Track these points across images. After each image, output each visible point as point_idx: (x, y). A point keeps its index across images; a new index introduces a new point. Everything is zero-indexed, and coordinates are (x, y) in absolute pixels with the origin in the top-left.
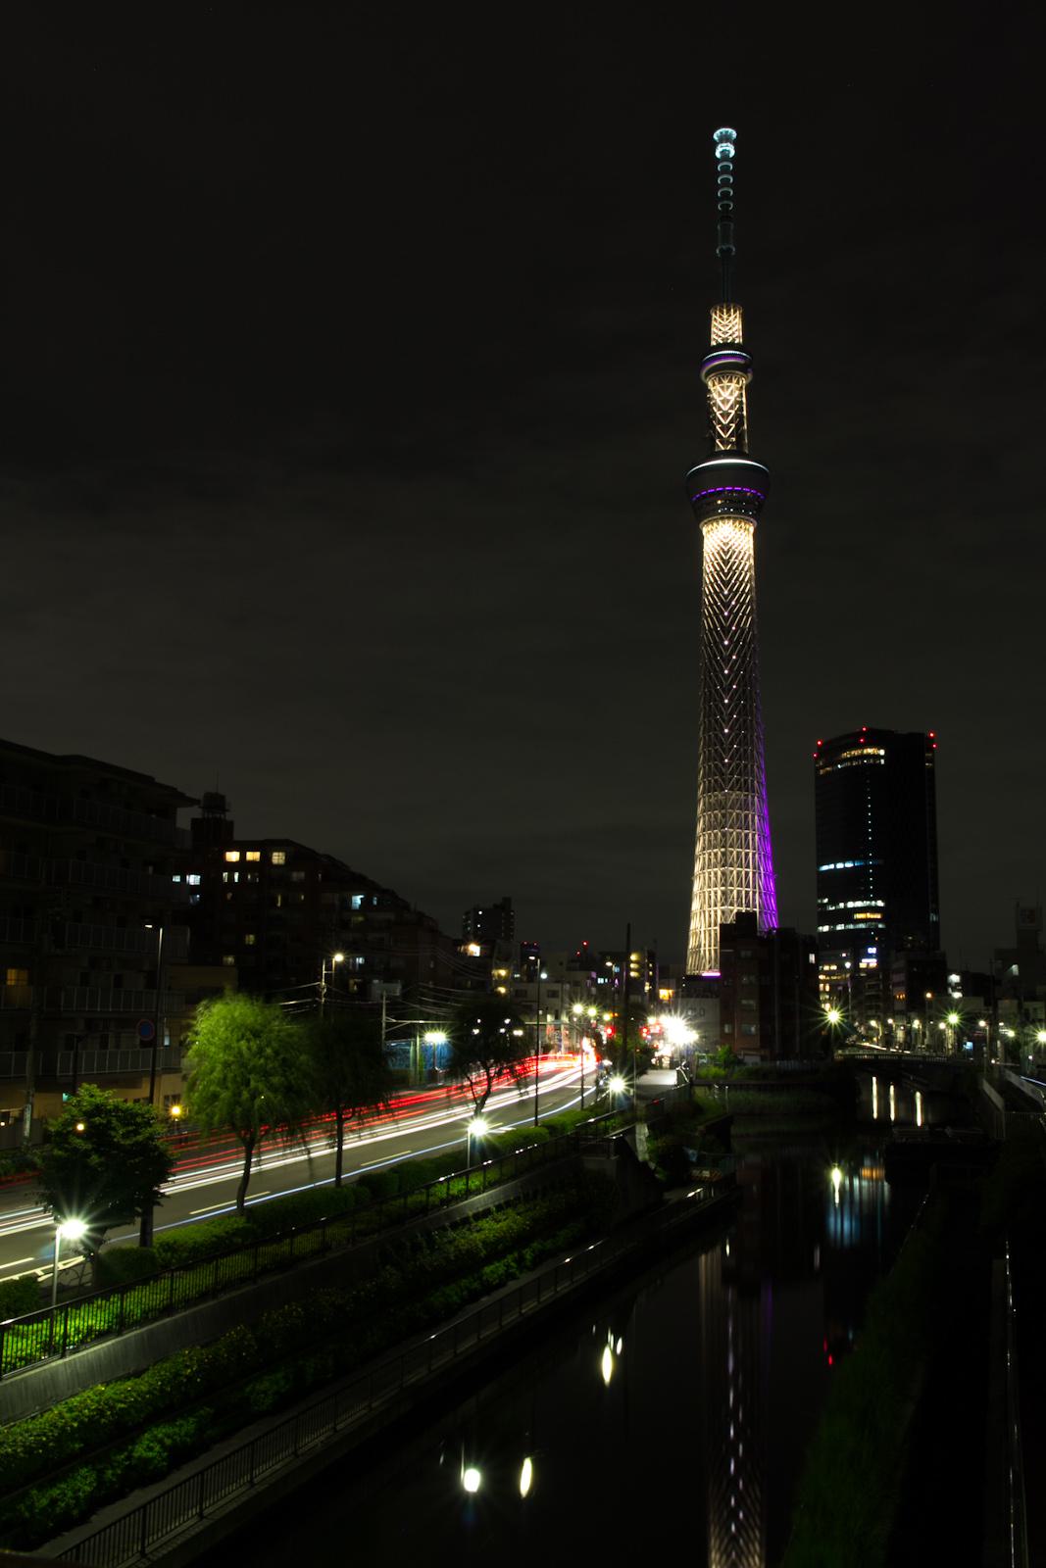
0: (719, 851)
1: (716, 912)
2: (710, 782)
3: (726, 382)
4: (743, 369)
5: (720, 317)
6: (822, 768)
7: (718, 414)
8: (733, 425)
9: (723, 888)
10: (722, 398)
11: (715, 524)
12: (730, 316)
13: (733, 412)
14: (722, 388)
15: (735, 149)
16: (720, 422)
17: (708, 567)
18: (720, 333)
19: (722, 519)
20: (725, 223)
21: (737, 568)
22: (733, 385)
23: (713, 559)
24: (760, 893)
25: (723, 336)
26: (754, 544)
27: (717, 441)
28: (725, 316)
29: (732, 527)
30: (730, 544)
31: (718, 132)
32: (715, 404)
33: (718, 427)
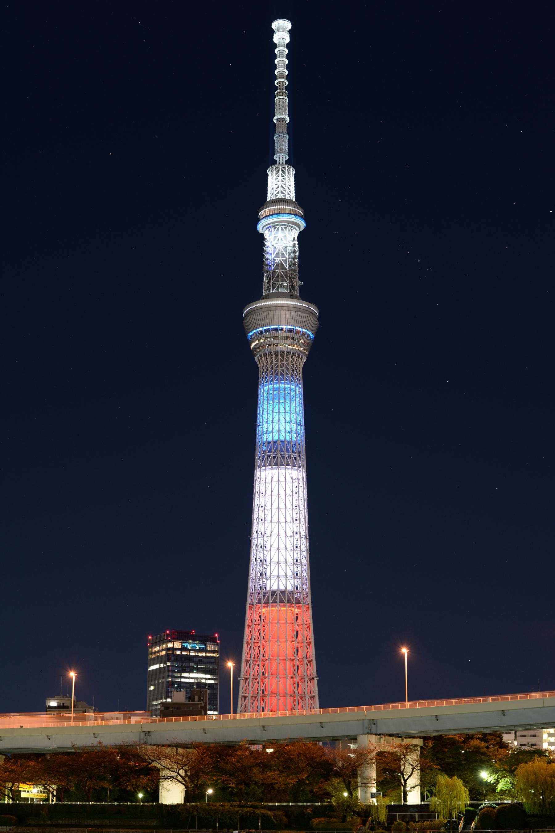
12: (278, 176)
20: (281, 97)
31: (275, 25)
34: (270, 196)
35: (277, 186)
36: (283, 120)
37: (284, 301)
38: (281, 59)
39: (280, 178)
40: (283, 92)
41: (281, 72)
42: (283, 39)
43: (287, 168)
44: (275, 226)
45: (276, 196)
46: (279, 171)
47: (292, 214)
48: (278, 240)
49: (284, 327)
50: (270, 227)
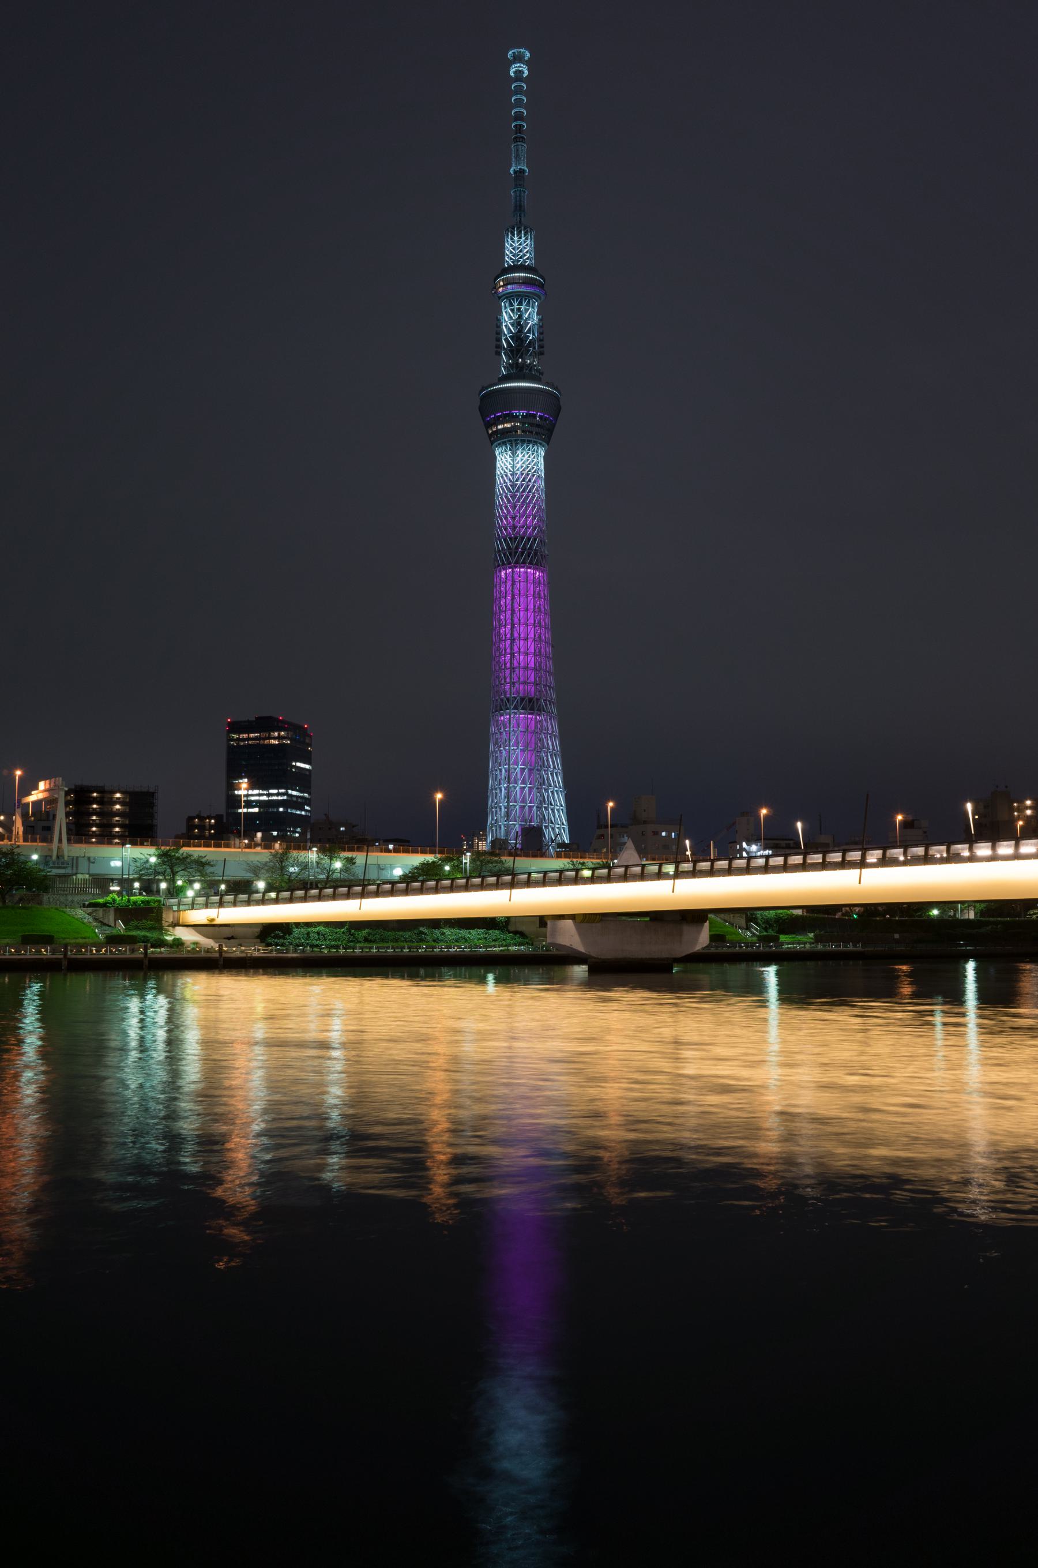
5: (512, 239)
12: (520, 238)
14: (512, 310)
15: (528, 70)
17: (499, 490)
20: (519, 144)
21: (524, 491)
23: (502, 482)
28: (516, 238)
34: (508, 260)
36: (522, 171)
37: (524, 382)
38: (518, 97)
40: (520, 137)
41: (519, 113)
42: (520, 71)
43: (529, 229)
44: (519, 296)
45: (518, 261)
47: (535, 285)
48: (530, 314)
49: (514, 412)
50: (513, 296)
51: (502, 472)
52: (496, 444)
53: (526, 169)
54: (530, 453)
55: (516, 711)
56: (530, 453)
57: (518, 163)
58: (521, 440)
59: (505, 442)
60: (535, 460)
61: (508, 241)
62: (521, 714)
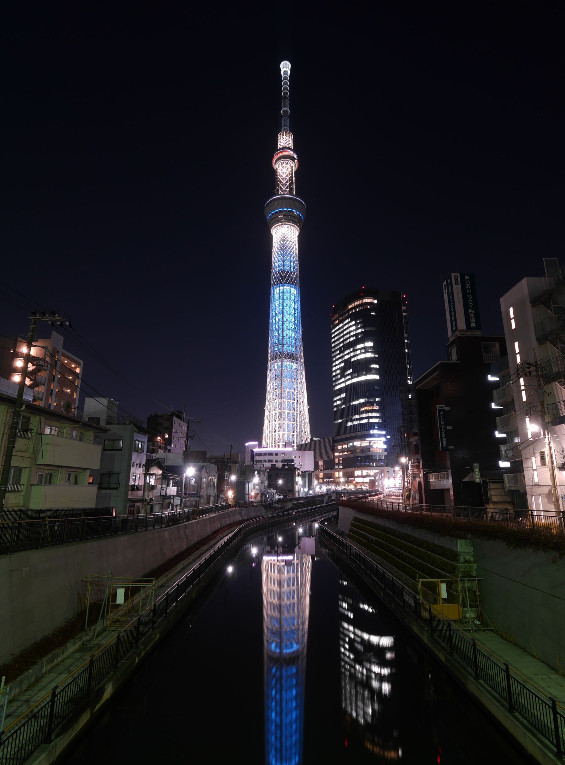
0: (278, 391)
1: (276, 424)
2: (273, 354)
3: (284, 165)
4: (293, 159)
5: (282, 137)
6: (335, 320)
7: (280, 179)
8: (288, 184)
9: (279, 411)
10: (283, 172)
11: (278, 228)
12: (287, 136)
13: (288, 178)
14: (283, 167)
16: (281, 182)
18: (282, 144)
19: (282, 225)
21: (289, 249)
22: (288, 166)
24: (300, 415)
25: (283, 145)
26: (298, 240)
27: (280, 191)
28: (285, 137)
29: (286, 230)
30: (286, 236)
32: (279, 175)
33: (280, 185)
35: (286, 142)
36: (287, 111)
39: (288, 138)
46: (287, 134)
51: (277, 240)
52: (274, 227)
53: (288, 109)
54: (292, 231)
55: (285, 359)
56: (292, 231)
57: (285, 106)
58: (288, 225)
59: (279, 225)
60: (294, 235)
61: (280, 139)
62: (287, 362)
